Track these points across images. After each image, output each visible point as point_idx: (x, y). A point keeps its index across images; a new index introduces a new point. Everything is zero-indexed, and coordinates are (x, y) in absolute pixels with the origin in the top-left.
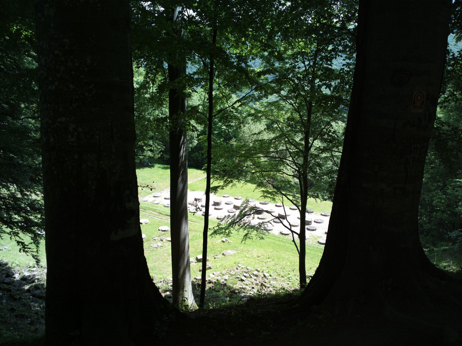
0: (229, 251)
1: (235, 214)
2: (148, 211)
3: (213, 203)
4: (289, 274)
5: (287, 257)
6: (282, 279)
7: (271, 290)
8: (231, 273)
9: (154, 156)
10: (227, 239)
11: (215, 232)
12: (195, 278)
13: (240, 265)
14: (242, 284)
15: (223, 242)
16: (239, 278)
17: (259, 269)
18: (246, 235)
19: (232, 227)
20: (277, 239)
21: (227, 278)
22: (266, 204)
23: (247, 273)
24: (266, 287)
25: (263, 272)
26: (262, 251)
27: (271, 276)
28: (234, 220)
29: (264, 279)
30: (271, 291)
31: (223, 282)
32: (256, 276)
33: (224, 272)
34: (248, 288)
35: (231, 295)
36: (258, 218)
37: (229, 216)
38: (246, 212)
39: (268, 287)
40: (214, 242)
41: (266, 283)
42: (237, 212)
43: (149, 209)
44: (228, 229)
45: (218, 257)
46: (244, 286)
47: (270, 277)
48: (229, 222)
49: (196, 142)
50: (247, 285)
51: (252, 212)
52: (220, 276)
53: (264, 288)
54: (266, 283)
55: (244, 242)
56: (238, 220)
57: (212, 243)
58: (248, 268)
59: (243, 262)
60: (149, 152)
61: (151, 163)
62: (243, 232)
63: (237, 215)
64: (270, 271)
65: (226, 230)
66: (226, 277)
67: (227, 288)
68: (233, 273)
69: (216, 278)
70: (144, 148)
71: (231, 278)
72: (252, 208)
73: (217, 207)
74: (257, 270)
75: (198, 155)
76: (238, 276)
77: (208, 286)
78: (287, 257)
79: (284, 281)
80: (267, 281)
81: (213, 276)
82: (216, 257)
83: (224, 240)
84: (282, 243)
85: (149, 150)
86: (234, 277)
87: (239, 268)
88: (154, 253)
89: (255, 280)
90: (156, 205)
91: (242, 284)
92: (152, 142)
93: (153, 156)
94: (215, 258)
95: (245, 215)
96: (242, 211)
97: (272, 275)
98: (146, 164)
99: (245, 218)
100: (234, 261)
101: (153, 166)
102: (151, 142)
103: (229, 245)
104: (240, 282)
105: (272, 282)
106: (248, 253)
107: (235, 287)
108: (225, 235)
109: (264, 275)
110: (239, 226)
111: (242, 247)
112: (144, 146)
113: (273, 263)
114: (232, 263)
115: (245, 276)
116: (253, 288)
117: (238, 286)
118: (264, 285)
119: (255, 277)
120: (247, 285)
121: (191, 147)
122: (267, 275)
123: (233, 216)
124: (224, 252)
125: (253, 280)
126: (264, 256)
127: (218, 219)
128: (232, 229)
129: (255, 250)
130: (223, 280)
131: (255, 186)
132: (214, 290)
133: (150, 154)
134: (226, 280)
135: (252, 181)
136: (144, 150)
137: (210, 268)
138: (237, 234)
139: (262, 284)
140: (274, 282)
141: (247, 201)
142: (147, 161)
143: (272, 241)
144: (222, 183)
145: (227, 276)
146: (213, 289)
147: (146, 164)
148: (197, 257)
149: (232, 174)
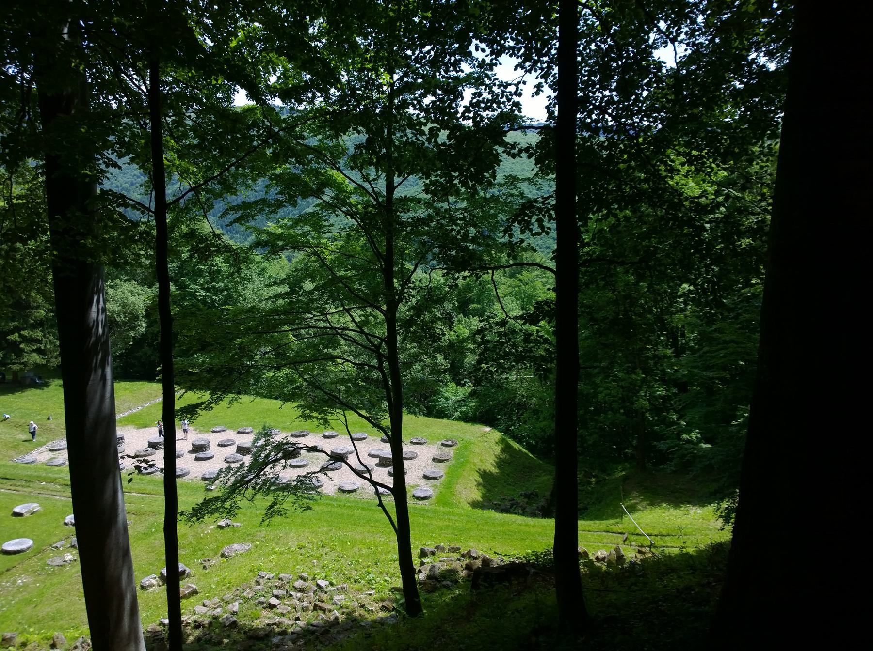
0: (235, 546)
1: (243, 464)
2: (36, 484)
3: (190, 448)
4: (369, 573)
5: (358, 537)
6: (356, 586)
7: (338, 614)
8: (245, 594)
9: (48, 362)
10: (229, 522)
11: (198, 513)
12: (161, 624)
13: (263, 574)
14: (271, 615)
15: (220, 527)
16: (262, 603)
17: (305, 575)
18: (271, 507)
19: (239, 494)
20: (335, 504)
21: (235, 609)
22: (303, 436)
23: (279, 588)
24: (324, 611)
25: (314, 579)
26: (307, 534)
27: (332, 584)
28: (243, 477)
29: (319, 594)
30: (336, 618)
31: (227, 618)
32: (301, 590)
33: (228, 596)
34: (286, 621)
35: (250, 646)
36: (291, 466)
37: (229, 468)
38: (267, 456)
39: (330, 611)
40: (200, 531)
41: (323, 601)
42: (248, 460)
43: (40, 479)
44: (228, 497)
45: (213, 562)
46: (277, 619)
47: (330, 588)
48: (229, 484)
49: (145, 325)
50: (283, 615)
51: (280, 455)
52: (220, 606)
53: (321, 613)
54: (323, 601)
55: (267, 522)
56: (250, 477)
57: (196, 535)
58: (281, 575)
59: (270, 565)
60: (34, 354)
61: (40, 378)
62: (263, 501)
63: (247, 464)
64: (329, 573)
65: (223, 502)
66: (235, 606)
67: (239, 632)
68: (248, 594)
69: (211, 613)
70: (22, 346)
71: (246, 606)
72: (279, 447)
73: (201, 455)
74: (301, 578)
75: (150, 352)
76: (262, 599)
77: (192, 636)
78: (358, 537)
79: (360, 590)
80: (325, 597)
81: (205, 609)
82: (207, 564)
83: (222, 523)
84: (346, 511)
85: (34, 351)
86: (252, 602)
87: (261, 581)
88: (55, 580)
89: (299, 599)
90: (56, 469)
91: (271, 615)
92: (40, 334)
93: (44, 362)
94: (204, 567)
95: (266, 464)
96: (256, 456)
97: (334, 581)
98: (28, 381)
99: (268, 469)
100: (249, 567)
101: (47, 385)
102: (38, 334)
103: (235, 532)
104: (264, 612)
105: (336, 598)
106: (277, 544)
107: (256, 623)
108: (224, 515)
109: (318, 586)
110: (254, 488)
111: (264, 531)
112: (21, 343)
113: (333, 555)
114: (245, 571)
115: (277, 597)
116: (297, 619)
117: (264, 620)
118: (321, 609)
119: (299, 595)
120: (283, 615)
121: (133, 338)
122: (323, 583)
123: (239, 469)
124: (225, 549)
125: (295, 602)
126: (312, 542)
127: (204, 479)
128: (239, 498)
129: (292, 534)
130: (228, 615)
131: (278, 403)
132: (209, 641)
133: (36, 358)
134: (234, 613)
135: (273, 392)
136: (22, 350)
137: (195, 592)
138: (251, 507)
139: (316, 606)
140: (340, 597)
141: (266, 433)
142: (32, 374)
143: (326, 509)
144: (206, 396)
145: (237, 603)
146: (207, 641)
147: (28, 381)
148: (161, 574)
149: (228, 380)
